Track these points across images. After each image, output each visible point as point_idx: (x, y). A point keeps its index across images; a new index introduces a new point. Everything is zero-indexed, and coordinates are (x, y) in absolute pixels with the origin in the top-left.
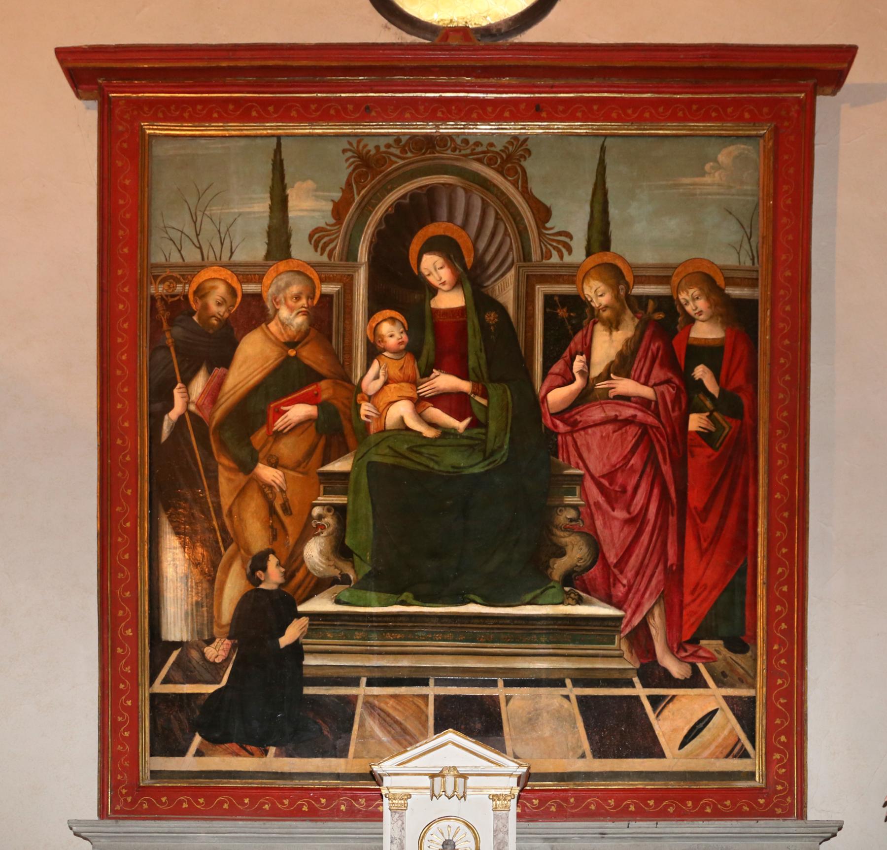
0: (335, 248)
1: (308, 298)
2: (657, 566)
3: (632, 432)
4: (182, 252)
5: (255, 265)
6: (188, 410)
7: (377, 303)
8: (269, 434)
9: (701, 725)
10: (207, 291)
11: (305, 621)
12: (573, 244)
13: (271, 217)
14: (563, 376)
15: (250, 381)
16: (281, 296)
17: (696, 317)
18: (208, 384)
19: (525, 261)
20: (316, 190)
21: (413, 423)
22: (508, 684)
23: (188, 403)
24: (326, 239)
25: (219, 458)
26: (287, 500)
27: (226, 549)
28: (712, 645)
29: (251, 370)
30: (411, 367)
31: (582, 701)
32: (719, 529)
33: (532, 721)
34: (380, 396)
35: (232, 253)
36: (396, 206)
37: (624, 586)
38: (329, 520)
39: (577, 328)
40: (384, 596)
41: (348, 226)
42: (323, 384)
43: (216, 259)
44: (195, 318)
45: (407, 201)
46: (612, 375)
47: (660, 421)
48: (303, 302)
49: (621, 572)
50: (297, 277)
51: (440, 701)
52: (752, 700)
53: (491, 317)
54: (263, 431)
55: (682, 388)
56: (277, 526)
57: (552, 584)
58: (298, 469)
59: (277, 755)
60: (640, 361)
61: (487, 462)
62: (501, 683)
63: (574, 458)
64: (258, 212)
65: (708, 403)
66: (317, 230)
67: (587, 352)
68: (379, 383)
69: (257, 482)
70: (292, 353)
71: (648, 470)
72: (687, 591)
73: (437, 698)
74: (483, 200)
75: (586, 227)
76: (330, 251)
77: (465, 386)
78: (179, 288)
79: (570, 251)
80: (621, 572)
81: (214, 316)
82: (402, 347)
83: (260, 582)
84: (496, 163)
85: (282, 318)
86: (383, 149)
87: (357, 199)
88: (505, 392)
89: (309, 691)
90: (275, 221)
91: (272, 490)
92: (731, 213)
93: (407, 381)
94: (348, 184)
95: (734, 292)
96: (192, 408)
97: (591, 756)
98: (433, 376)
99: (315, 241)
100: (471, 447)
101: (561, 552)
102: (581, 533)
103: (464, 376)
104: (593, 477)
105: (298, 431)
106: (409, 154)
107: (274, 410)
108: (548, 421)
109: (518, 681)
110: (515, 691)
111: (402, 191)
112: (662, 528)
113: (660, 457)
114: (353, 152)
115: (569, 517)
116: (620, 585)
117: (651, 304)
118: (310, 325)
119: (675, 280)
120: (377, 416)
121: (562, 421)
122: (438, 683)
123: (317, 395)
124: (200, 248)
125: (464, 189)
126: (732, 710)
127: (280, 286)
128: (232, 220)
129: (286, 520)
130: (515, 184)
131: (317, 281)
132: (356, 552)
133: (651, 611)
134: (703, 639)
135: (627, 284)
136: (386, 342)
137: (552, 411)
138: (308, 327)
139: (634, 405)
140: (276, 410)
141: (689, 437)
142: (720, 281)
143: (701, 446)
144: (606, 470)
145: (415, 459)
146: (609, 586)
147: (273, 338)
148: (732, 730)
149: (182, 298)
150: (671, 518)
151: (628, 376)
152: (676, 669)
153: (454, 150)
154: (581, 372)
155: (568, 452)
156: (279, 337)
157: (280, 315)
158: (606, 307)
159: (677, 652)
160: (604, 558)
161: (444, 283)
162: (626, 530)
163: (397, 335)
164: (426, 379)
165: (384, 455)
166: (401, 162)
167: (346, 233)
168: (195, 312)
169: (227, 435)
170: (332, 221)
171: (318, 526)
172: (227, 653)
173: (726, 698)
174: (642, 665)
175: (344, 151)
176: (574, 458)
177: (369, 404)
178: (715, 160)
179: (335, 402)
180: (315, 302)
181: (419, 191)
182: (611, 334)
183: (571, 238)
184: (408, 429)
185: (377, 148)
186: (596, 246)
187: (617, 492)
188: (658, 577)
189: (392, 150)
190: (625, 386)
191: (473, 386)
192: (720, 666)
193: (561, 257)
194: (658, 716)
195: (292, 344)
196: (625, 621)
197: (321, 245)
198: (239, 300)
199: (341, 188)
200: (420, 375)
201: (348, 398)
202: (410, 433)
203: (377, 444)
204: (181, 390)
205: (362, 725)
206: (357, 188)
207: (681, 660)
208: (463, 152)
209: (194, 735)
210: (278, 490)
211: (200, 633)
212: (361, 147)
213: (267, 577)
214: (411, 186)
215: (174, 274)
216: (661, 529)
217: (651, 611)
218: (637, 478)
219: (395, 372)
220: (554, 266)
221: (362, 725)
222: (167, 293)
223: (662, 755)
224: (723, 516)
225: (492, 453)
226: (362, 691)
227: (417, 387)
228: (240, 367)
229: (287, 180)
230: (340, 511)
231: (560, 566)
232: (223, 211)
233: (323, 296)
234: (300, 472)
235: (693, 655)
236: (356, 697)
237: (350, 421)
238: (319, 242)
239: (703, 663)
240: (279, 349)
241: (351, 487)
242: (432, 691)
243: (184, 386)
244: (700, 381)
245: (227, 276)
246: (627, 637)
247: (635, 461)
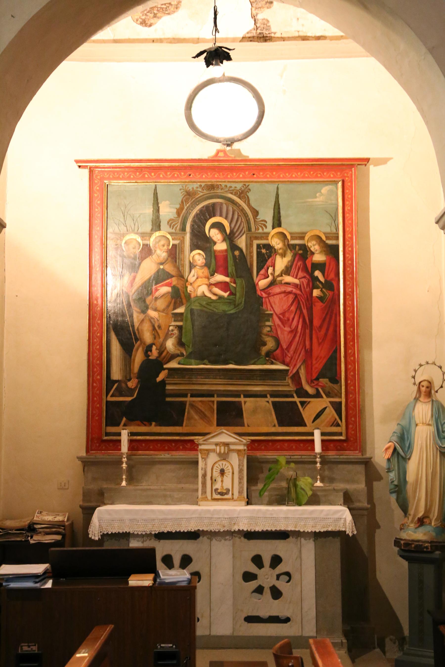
2: (302, 350)
3: (291, 297)
7: (194, 247)
9: (321, 413)
11: (166, 371)
12: (267, 225)
14: (264, 275)
16: (157, 245)
17: (315, 252)
19: (249, 231)
20: (170, 204)
21: (208, 294)
22: (245, 396)
27: (136, 343)
28: (324, 381)
30: (206, 271)
31: (274, 404)
32: (326, 335)
33: (255, 411)
37: (289, 357)
38: (176, 332)
39: (269, 257)
40: (197, 361)
42: (174, 279)
45: (205, 208)
46: (283, 275)
47: (302, 292)
49: (288, 352)
52: (340, 403)
53: (237, 253)
55: (310, 279)
56: (156, 334)
57: (261, 357)
59: (155, 426)
60: (294, 269)
61: (236, 309)
62: (242, 396)
63: (269, 307)
65: (320, 285)
66: (170, 220)
67: (274, 266)
70: (162, 267)
71: (298, 311)
72: (314, 359)
73: (218, 402)
74: (233, 208)
75: (272, 218)
77: (227, 279)
79: (266, 227)
80: (288, 352)
82: (203, 264)
83: (149, 356)
84: (237, 194)
87: (185, 208)
88: (242, 281)
89: (168, 399)
92: (327, 212)
94: (182, 202)
95: (330, 242)
97: (278, 426)
98: (215, 275)
100: (230, 303)
101: (265, 344)
102: (272, 336)
103: (227, 276)
104: (276, 314)
108: (259, 293)
109: (249, 395)
110: (247, 399)
112: (304, 334)
113: (302, 306)
115: (268, 330)
116: (288, 357)
117: (297, 247)
119: (306, 238)
121: (264, 292)
122: (219, 396)
123: (171, 283)
124: (126, 226)
125: (226, 204)
126: (333, 407)
129: (159, 331)
130: (245, 202)
132: (186, 344)
133: (300, 367)
134: (320, 378)
135: (288, 240)
137: (261, 289)
139: (291, 286)
141: (313, 299)
142: (324, 238)
143: (318, 302)
144: (281, 312)
146: (284, 357)
148: (333, 415)
150: (307, 330)
151: (289, 275)
152: (310, 390)
153: (222, 189)
154: (271, 274)
155: (267, 304)
158: (280, 249)
159: (311, 384)
160: (282, 347)
161: (219, 240)
162: (290, 335)
164: (212, 277)
170: (176, 216)
172: (136, 384)
173: (331, 402)
174: (297, 389)
176: (269, 307)
178: (321, 192)
179: (178, 286)
180: (170, 247)
182: (282, 259)
183: (266, 222)
184: (205, 296)
186: (276, 225)
187: (285, 320)
188: (303, 353)
190: (288, 279)
191: (230, 280)
192: (327, 390)
193: (263, 230)
194: (304, 409)
195: (162, 264)
196: (290, 371)
197: (172, 225)
201: (183, 284)
202: (206, 297)
203: (194, 302)
205: (189, 413)
206: (185, 203)
207: (312, 387)
208: (225, 190)
209: (123, 417)
211: (126, 377)
216: (303, 335)
217: (300, 367)
219: (200, 274)
220: (260, 233)
221: (189, 413)
223: (305, 425)
224: (327, 330)
225: (238, 305)
226: (189, 399)
229: (159, 201)
230: (180, 328)
231: (264, 349)
234: (164, 313)
235: (317, 385)
236: (186, 402)
239: (321, 388)
242: (216, 399)
244: (317, 277)
246: (291, 378)
247: (293, 308)
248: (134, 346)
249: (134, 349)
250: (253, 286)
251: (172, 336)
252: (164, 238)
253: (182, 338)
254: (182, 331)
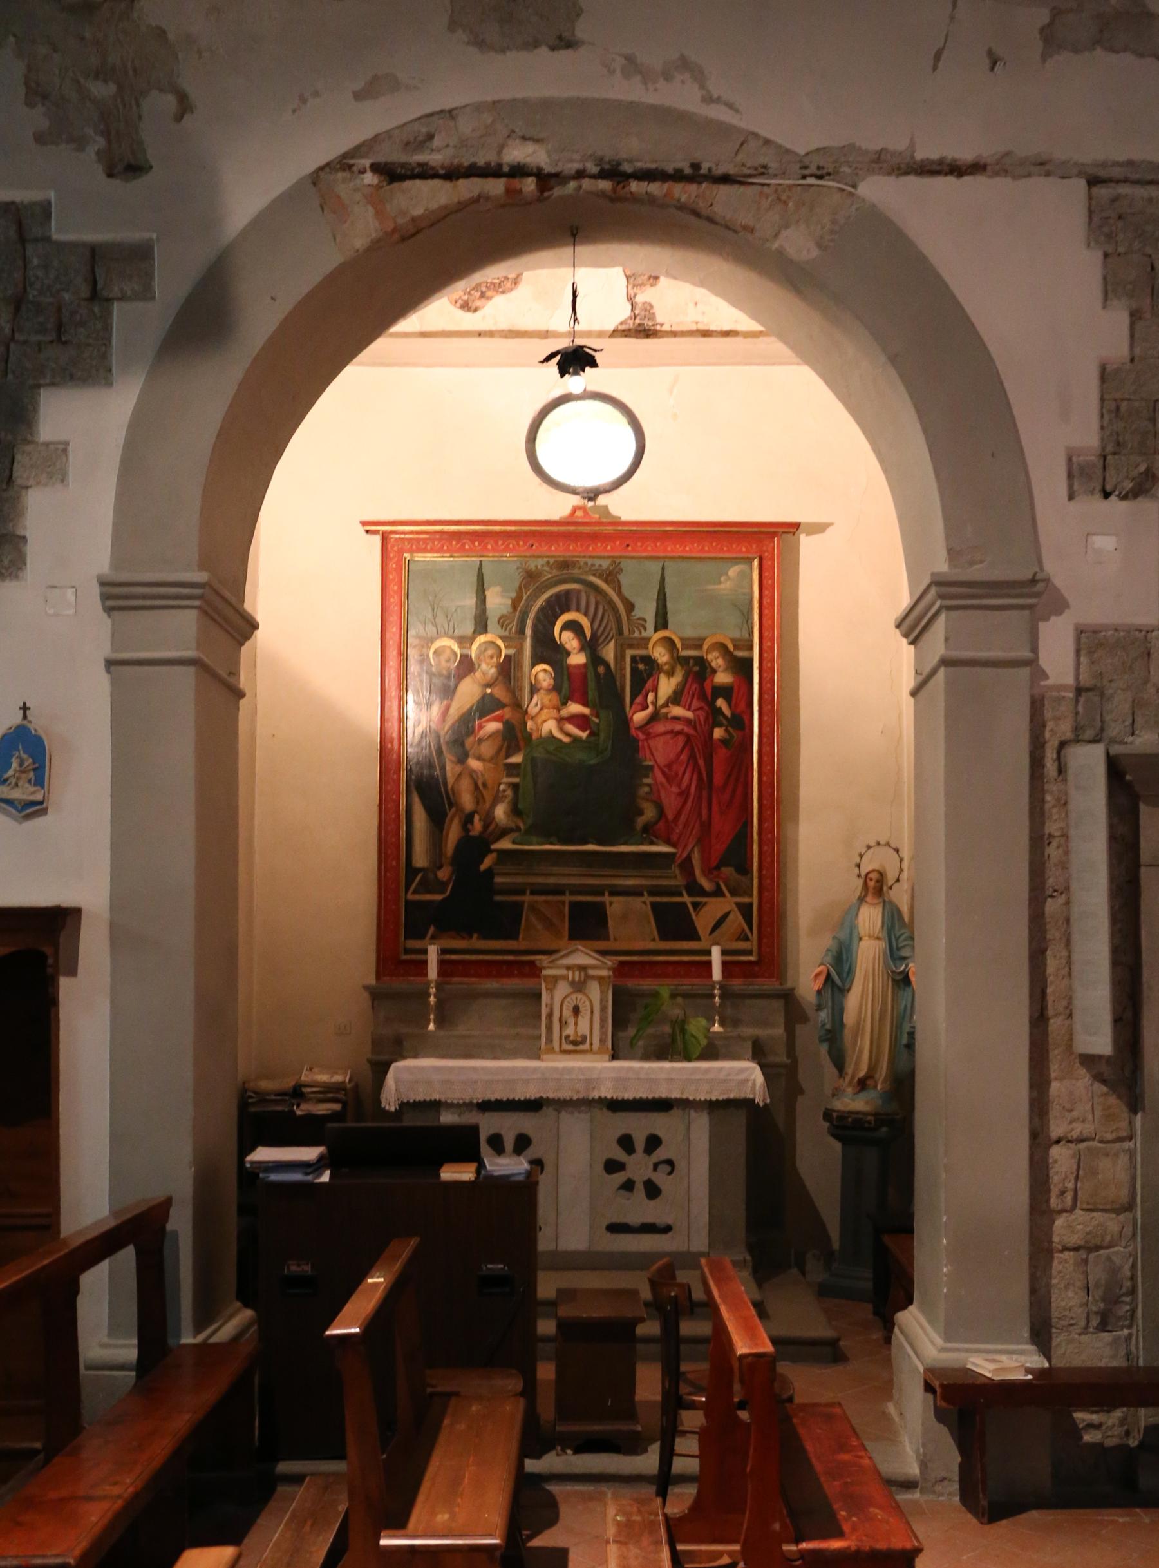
3: (681, 740)
11: (494, 855)
17: (717, 669)
21: (557, 734)
22: (612, 894)
28: (728, 871)
31: (654, 905)
38: (509, 793)
39: (650, 675)
46: (670, 705)
51: (573, 905)
52: (751, 904)
53: (601, 669)
62: (607, 894)
63: (648, 755)
65: (725, 722)
67: (655, 690)
77: (586, 711)
79: (645, 629)
82: (551, 687)
95: (740, 654)
102: (652, 801)
103: (585, 704)
104: (659, 766)
108: (633, 732)
109: (616, 892)
110: (615, 899)
113: (697, 754)
117: (691, 662)
119: (705, 647)
121: (641, 732)
122: (572, 893)
129: (485, 793)
130: (614, 589)
137: (636, 726)
142: (731, 647)
148: (740, 923)
154: (652, 703)
158: (666, 664)
160: (666, 816)
176: (648, 755)
182: (669, 679)
183: (646, 621)
188: (697, 825)
190: (677, 711)
193: (640, 633)
195: (489, 685)
196: (678, 855)
207: (710, 880)
217: (693, 849)
218: (685, 766)
219: (547, 702)
220: (635, 638)
223: (698, 939)
230: (515, 787)
231: (641, 821)
239: (724, 882)
242: (567, 898)
247: (684, 757)
250: (626, 722)
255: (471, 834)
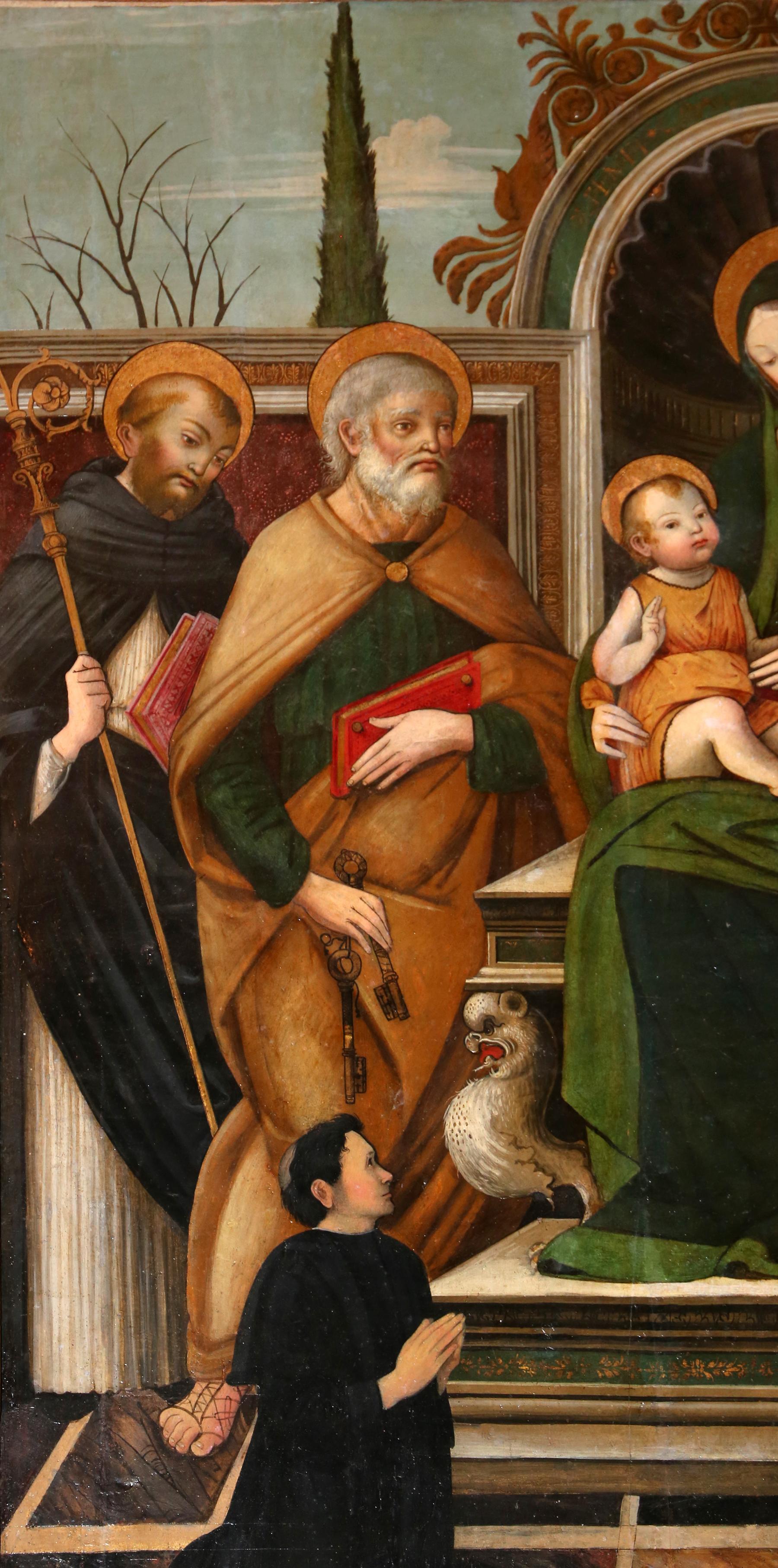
0: (507, 291)
1: (437, 425)
4: (83, 303)
5: (289, 339)
6: (108, 730)
8: (337, 793)
10: (156, 407)
13: (327, 213)
15: (281, 648)
18: (164, 657)
20: (452, 141)
23: (107, 710)
24: (482, 269)
25: (198, 859)
26: (395, 979)
29: (285, 619)
34: (647, 687)
35: (223, 308)
36: (671, 184)
41: (541, 234)
42: (486, 656)
43: (180, 324)
44: (124, 479)
45: (704, 168)
48: (425, 435)
50: (405, 369)
54: (324, 783)
56: (366, 1049)
58: (423, 890)
64: (291, 200)
66: (457, 246)
68: (642, 651)
69: (307, 927)
70: (398, 572)
76: (493, 299)
78: (77, 400)
81: (179, 475)
82: (704, 554)
85: (366, 481)
86: (631, 33)
87: (563, 164)
90: (339, 222)
91: (350, 950)
93: (722, 648)
94: (539, 125)
96: (120, 722)
99: (452, 274)
105: (423, 783)
106: (706, 48)
107: (351, 728)
111: (688, 143)
114: (550, 42)
118: (446, 499)
120: (640, 743)
123: (470, 686)
124: (134, 293)
127: (359, 396)
128: (220, 219)
129: (389, 1030)
131: (460, 381)
136: (656, 541)
138: (441, 503)
140: (358, 727)
145: (751, 859)
147: (344, 534)
149: (85, 426)
156: (360, 528)
157: (361, 472)
163: (688, 523)
165: (665, 849)
166: (683, 68)
167: (536, 254)
168: (124, 464)
169: (221, 795)
170: (497, 222)
171: (483, 1049)
175: (524, 39)
177: (617, 710)
179: (518, 703)
180: (458, 435)
181: (736, 144)
184: (727, 776)
185: (616, 30)
189: (657, 36)
197: (467, 284)
198: (245, 430)
199: (520, 137)
200: (757, 628)
201: (557, 695)
202: (733, 787)
203: (642, 819)
204: (87, 675)
206: (562, 135)
210: (368, 949)
212: (569, 29)
213: (341, 1197)
214: (714, 130)
215: (61, 363)
222: (44, 413)
227: (749, 661)
228: (252, 613)
229: (369, 117)
232: (193, 196)
233: (479, 420)
234: (428, 899)
237: (564, 754)
238: (464, 276)
240: (363, 562)
241: (574, 940)
243: (96, 664)
245: (212, 369)
248: (206, 1136)
249: (204, 1168)
251: (488, 1062)
252: (414, 372)
253: (559, 1079)
254: (559, 1027)
255: (328, 1225)
